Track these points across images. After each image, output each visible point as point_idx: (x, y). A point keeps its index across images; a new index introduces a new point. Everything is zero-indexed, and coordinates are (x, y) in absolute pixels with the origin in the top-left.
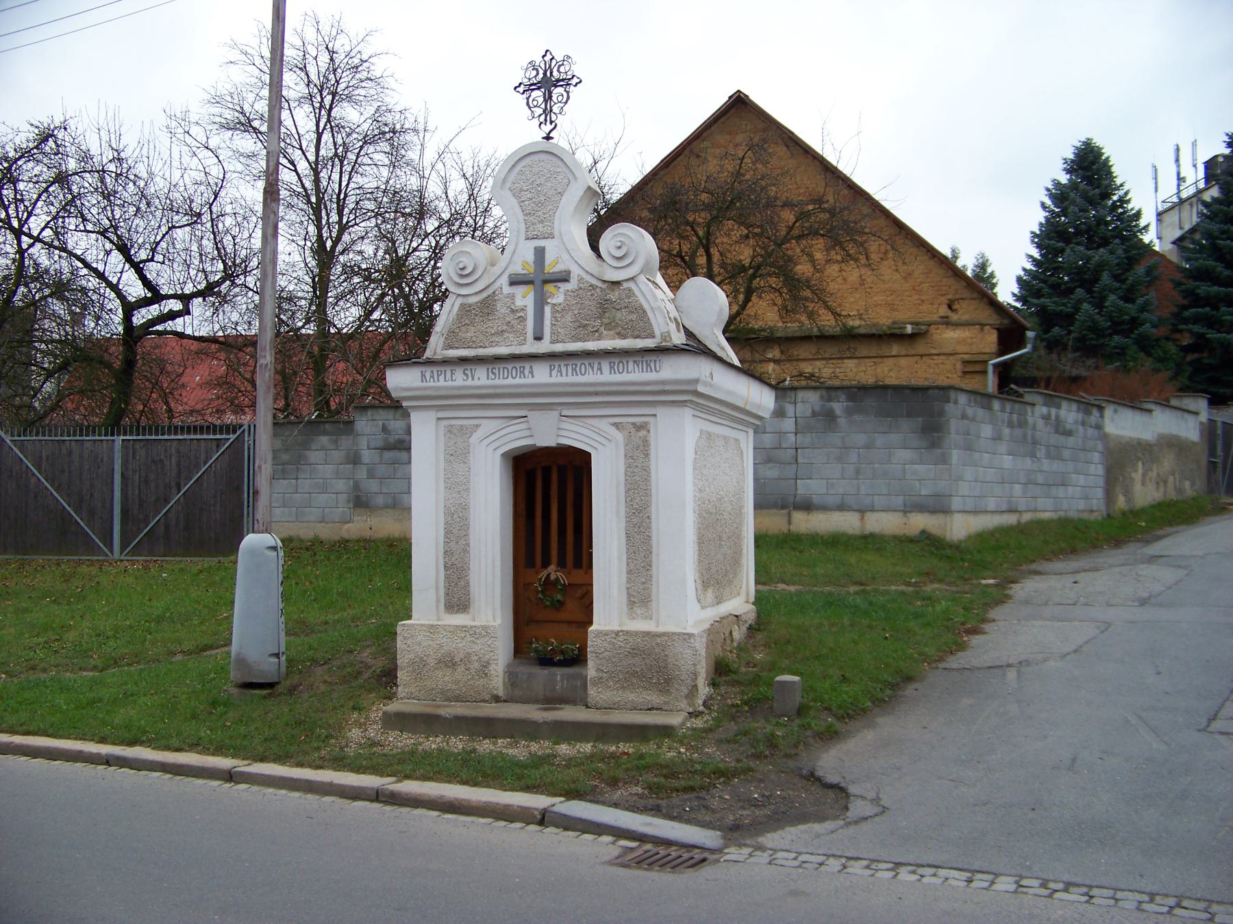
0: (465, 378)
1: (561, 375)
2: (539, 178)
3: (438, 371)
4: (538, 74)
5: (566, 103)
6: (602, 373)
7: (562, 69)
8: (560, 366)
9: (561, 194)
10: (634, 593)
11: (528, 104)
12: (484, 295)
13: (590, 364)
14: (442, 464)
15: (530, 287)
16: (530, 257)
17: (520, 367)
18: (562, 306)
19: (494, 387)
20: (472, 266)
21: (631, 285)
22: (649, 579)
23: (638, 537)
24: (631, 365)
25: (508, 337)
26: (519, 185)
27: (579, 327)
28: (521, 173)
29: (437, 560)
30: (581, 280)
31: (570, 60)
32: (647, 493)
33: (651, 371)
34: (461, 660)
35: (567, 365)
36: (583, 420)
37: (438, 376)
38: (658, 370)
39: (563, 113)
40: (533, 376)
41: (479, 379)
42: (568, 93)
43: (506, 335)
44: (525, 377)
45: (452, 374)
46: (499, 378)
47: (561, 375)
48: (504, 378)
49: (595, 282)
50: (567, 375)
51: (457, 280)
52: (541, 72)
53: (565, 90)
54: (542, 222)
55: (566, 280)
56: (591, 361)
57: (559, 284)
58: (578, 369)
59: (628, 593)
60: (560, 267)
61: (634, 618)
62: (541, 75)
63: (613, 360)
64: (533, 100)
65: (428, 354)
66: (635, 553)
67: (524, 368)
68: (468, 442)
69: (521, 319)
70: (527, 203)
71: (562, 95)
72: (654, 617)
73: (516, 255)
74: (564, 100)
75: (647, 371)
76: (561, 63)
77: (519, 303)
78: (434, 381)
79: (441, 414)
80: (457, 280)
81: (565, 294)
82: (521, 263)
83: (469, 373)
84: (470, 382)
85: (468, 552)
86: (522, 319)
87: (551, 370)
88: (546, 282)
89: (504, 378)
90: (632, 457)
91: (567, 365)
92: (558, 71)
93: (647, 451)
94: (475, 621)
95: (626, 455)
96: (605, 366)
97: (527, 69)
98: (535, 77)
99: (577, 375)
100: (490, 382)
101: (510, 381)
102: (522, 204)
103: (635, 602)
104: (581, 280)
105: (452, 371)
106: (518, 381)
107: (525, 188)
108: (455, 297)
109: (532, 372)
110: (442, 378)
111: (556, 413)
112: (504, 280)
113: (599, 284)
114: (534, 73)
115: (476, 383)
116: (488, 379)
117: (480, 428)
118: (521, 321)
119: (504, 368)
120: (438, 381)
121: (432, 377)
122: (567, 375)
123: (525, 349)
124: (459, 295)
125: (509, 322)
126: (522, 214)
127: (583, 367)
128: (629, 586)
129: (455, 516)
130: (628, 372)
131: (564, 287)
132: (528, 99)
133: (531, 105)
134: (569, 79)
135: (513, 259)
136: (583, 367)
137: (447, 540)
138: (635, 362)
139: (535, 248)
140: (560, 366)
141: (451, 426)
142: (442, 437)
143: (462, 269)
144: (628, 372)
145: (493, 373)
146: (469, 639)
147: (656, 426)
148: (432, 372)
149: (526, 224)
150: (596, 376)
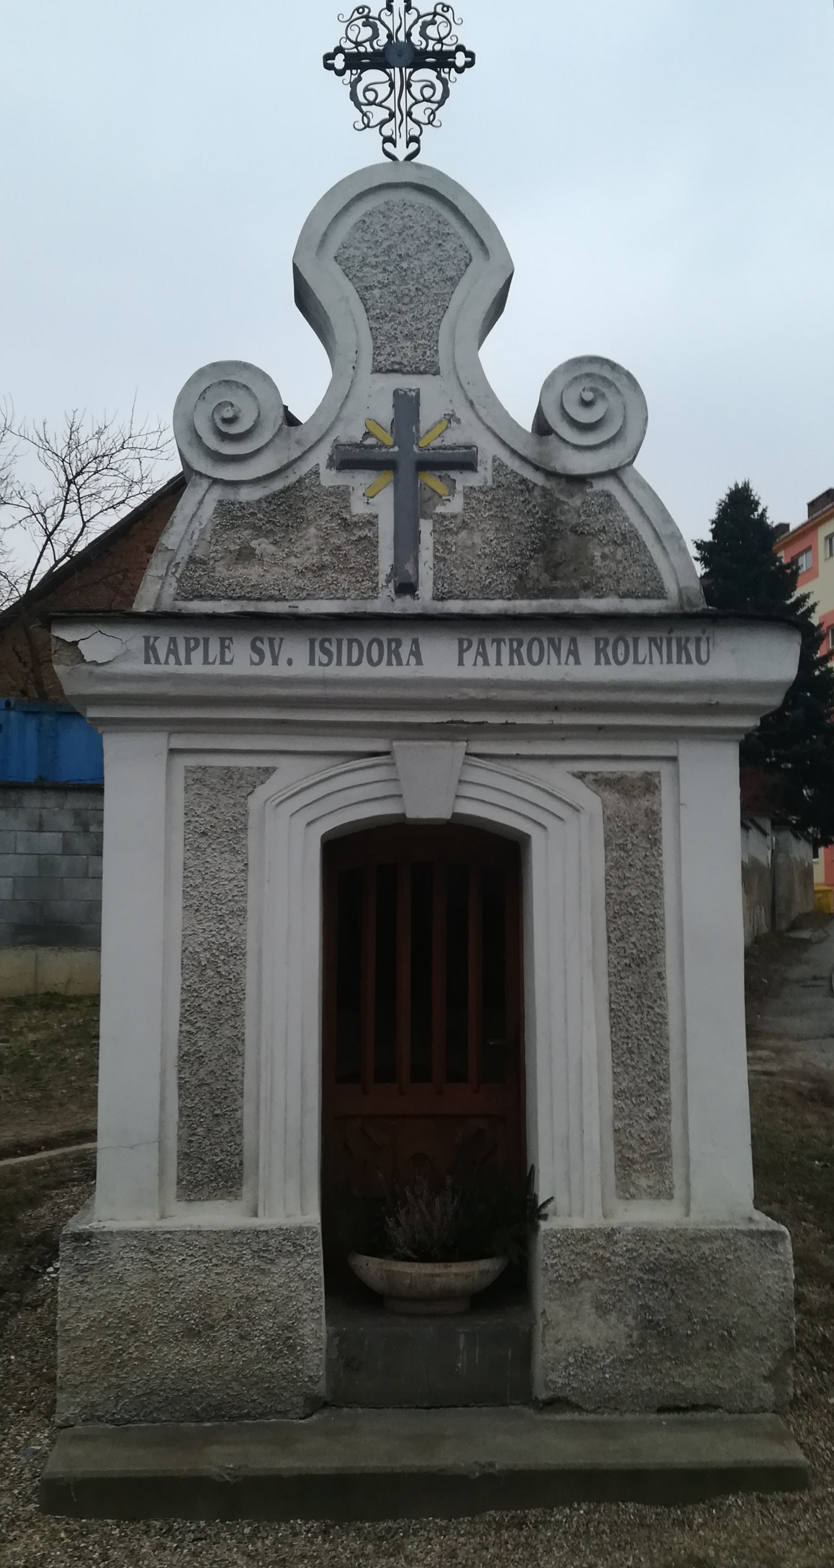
0: (256, 658)
1: (486, 663)
2: (404, 241)
3: (187, 640)
4: (376, 35)
5: (441, 103)
6: (577, 662)
7: (431, 31)
8: (482, 643)
9: (454, 281)
10: (633, 1142)
11: (353, 96)
12: (278, 485)
13: (551, 641)
14: (179, 854)
15: (387, 477)
16: (385, 413)
17: (390, 642)
18: (459, 521)
19: (324, 682)
20: (254, 417)
21: (610, 485)
22: (663, 1110)
23: (637, 1018)
24: (643, 649)
25: (335, 582)
26: (357, 253)
27: (498, 567)
28: (362, 225)
29: (163, 1073)
30: (499, 467)
31: (449, 15)
32: (656, 925)
33: (689, 661)
34: (229, 1316)
35: (498, 642)
36: (514, 764)
37: (189, 651)
38: (704, 659)
39: (435, 123)
40: (419, 662)
41: (290, 662)
42: (445, 83)
43: (330, 575)
44: (400, 663)
45: (223, 648)
46: (339, 663)
47: (486, 663)
48: (350, 663)
49: (528, 473)
50: (499, 663)
51: (212, 442)
52: (383, 33)
53: (439, 77)
54: (409, 337)
55: (468, 464)
56: (555, 635)
57: (454, 474)
58: (524, 650)
59: (618, 1142)
60: (454, 437)
61: (633, 1197)
62: (383, 39)
63: (602, 633)
64: (366, 89)
65: (144, 603)
66: (631, 1052)
67: (399, 643)
68: (244, 805)
69: (366, 543)
70: (376, 292)
71: (432, 86)
72: (678, 1193)
73: (350, 404)
74: (438, 97)
75: (679, 661)
76: (429, 18)
77: (358, 508)
78: (178, 662)
79: (179, 742)
80: (212, 442)
81: (466, 496)
82: (362, 422)
83: (266, 648)
84: (266, 669)
85: (241, 1055)
86: (372, 544)
87: (461, 651)
88: (425, 465)
89: (350, 663)
90: (622, 847)
91: (498, 642)
92: (423, 34)
93: (654, 833)
94: (255, 1214)
95: (607, 844)
96: (587, 649)
97: (350, 22)
98: (371, 40)
99: (521, 663)
100: (317, 671)
101: (365, 671)
102: (367, 295)
103: (633, 1161)
104: (499, 467)
105: (222, 641)
106: (384, 671)
107: (373, 261)
108: (205, 484)
109: (416, 653)
110: (197, 655)
111: (461, 746)
112: (321, 456)
113: (538, 479)
114: (367, 32)
115: (282, 670)
116: (312, 663)
117: (274, 778)
118: (365, 549)
119: (350, 642)
120: (188, 662)
121: (173, 651)
122: (499, 663)
123: (376, 606)
124: (215, 481)
125: (339, 548)
126: (365, 315)
127: (536, 647)
128: (619, 1125)
129: (210, 973)
130: (636, 661)
131: (463, 480)
132: (354, 85)
133: (362, 99)
134: (452, 54)
135: (345, 412)
136: (536, 647)
137: (186, 1027)
138: (652, 640)
139: (396, 393)
140: (482, 643)
141: (205, 769)
142: (180, 796)
143: (228, 421)
144: (636, 661)
145: (327, 652)
146: (251, 1263)
147: (678, 784)
148: (173, 640)
149: (375, 339)
150: (566, 669)
